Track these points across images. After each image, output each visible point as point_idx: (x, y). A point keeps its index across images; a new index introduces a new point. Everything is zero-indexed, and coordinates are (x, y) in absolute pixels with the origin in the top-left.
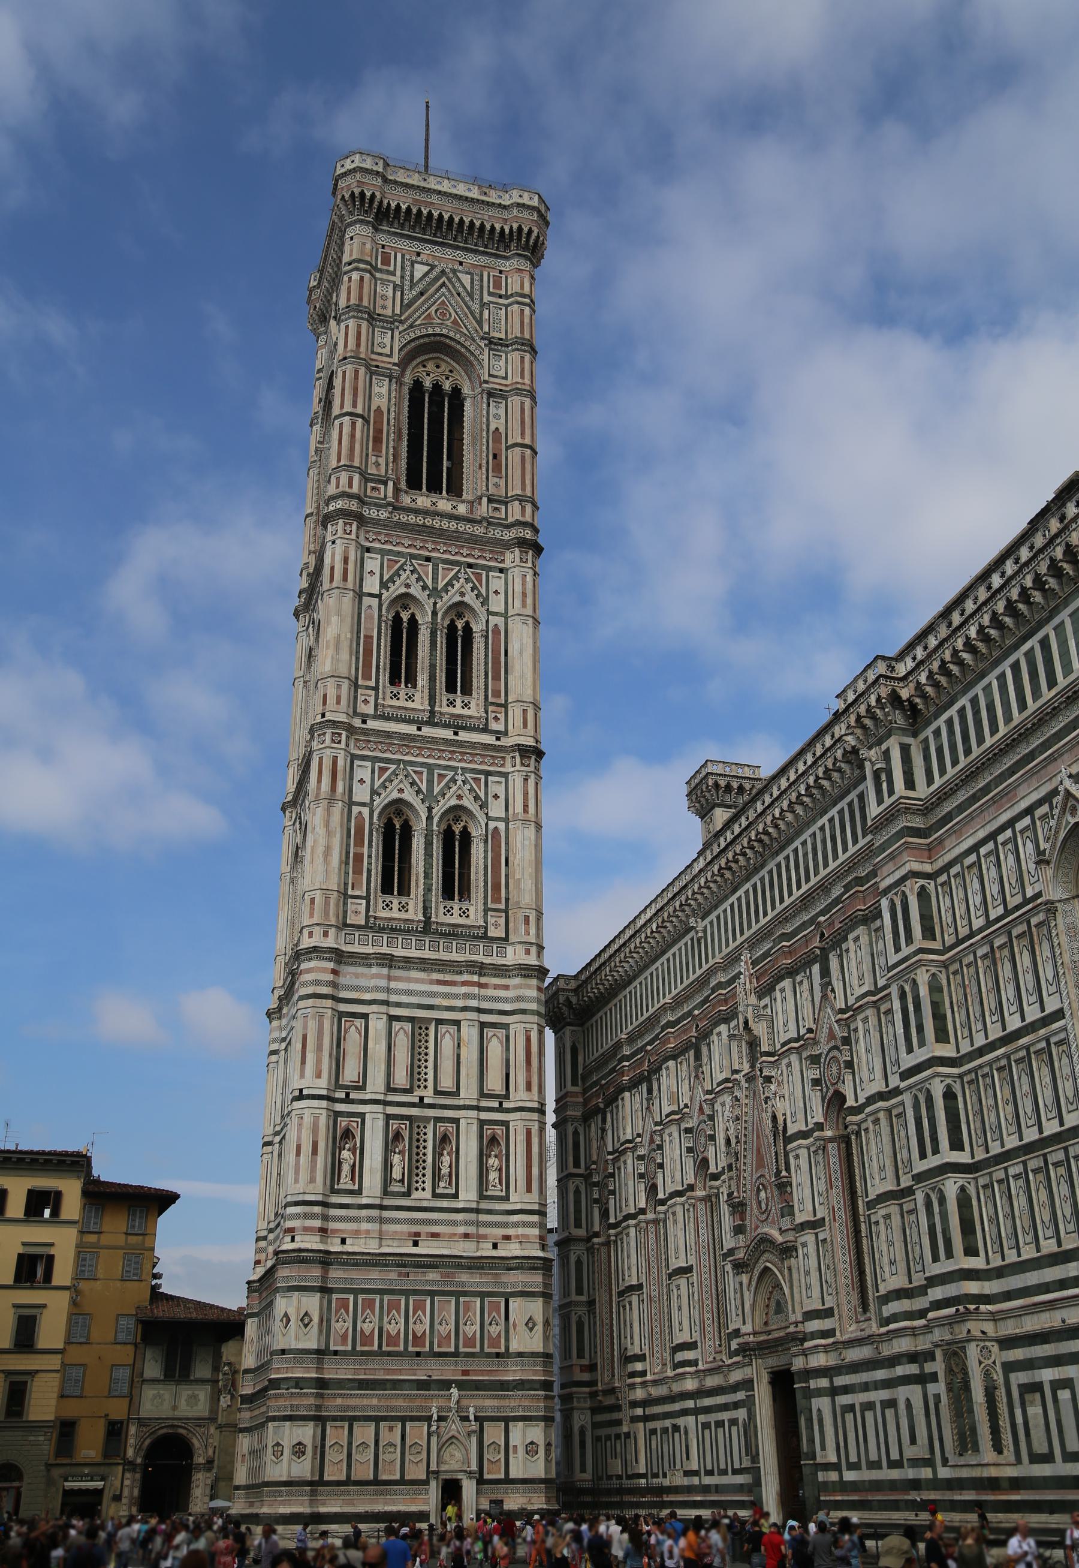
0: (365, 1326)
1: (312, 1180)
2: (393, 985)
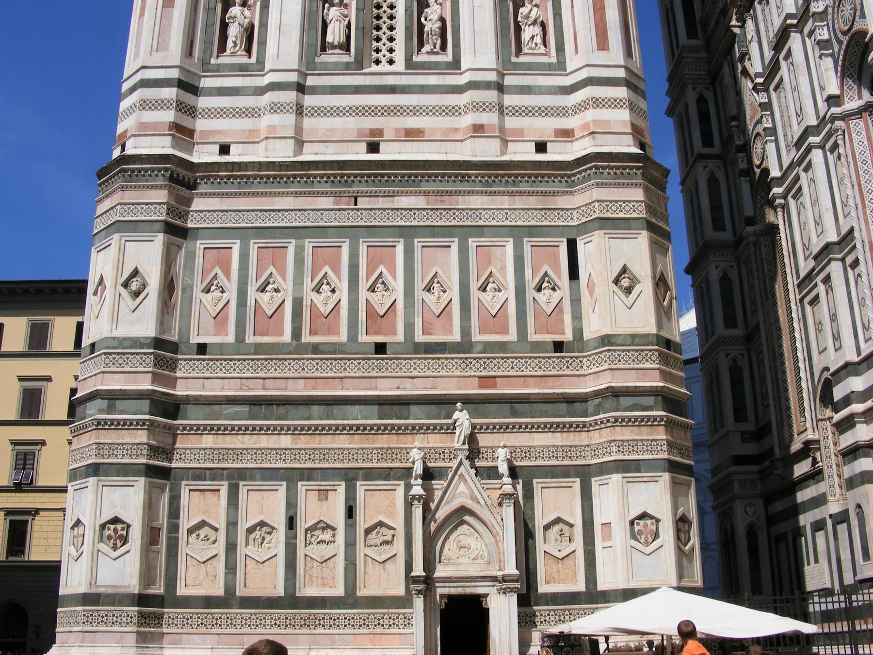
0: (265, 298)
1: (161, 46)
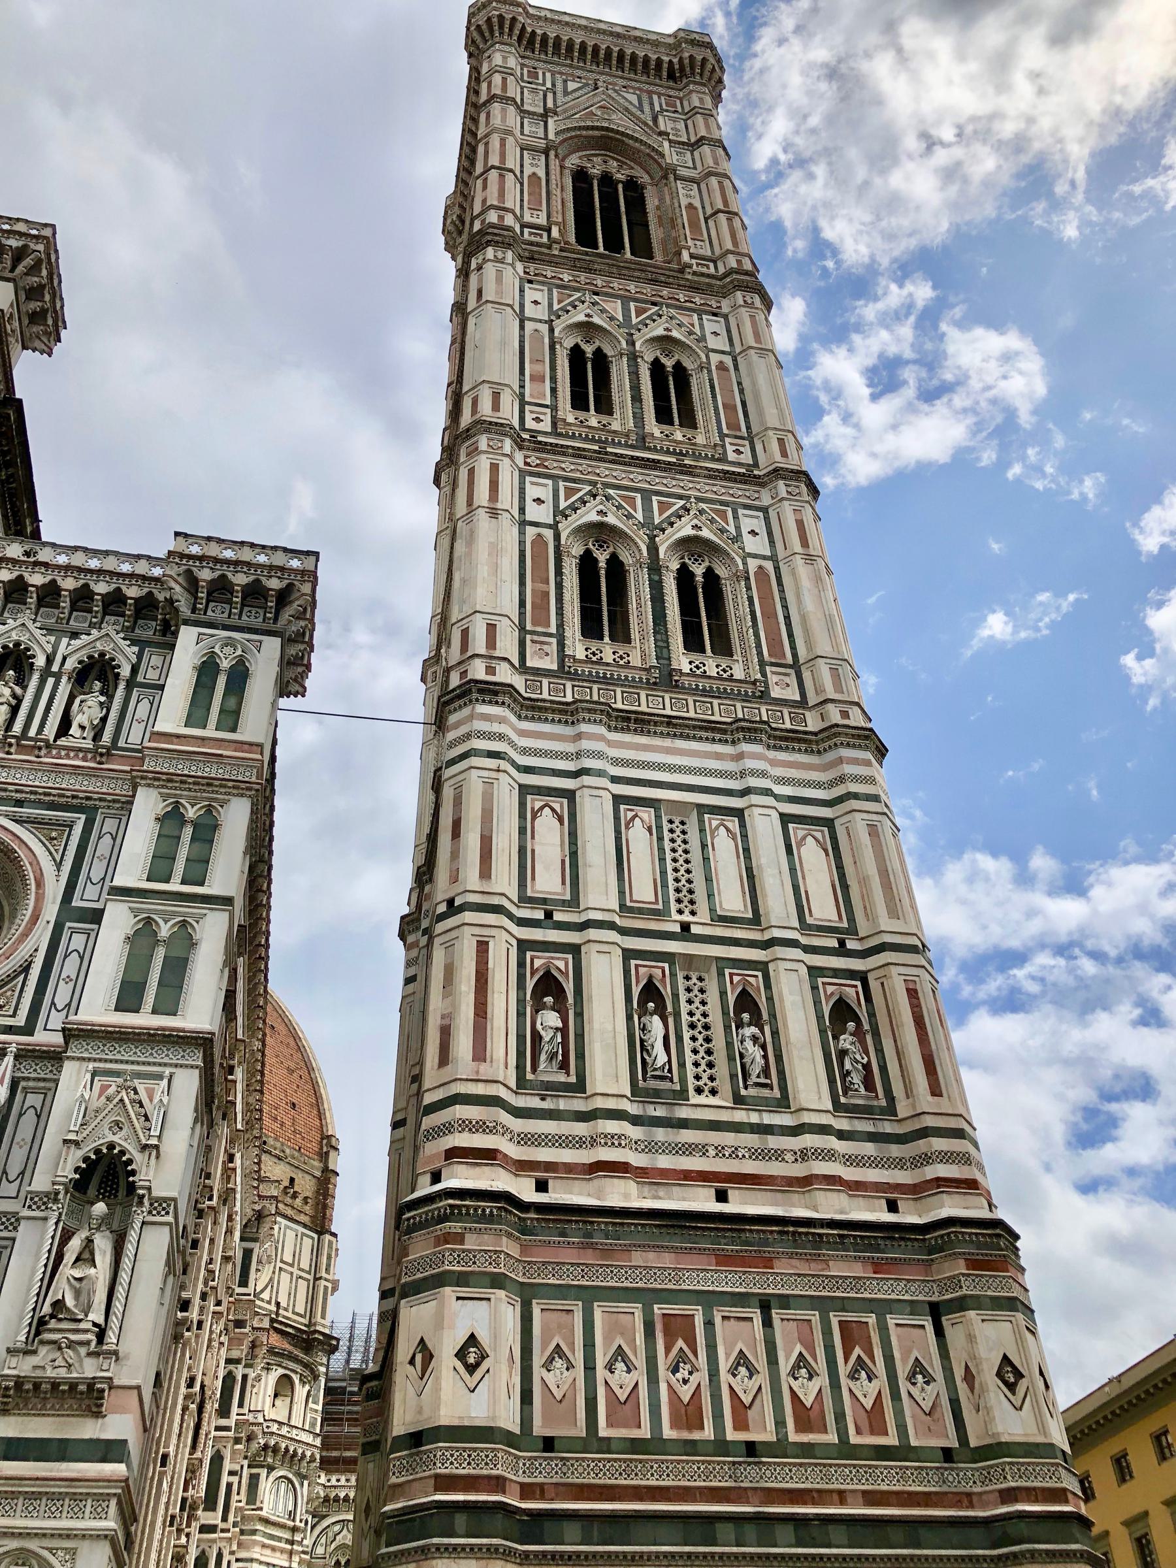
2: (613, 753)
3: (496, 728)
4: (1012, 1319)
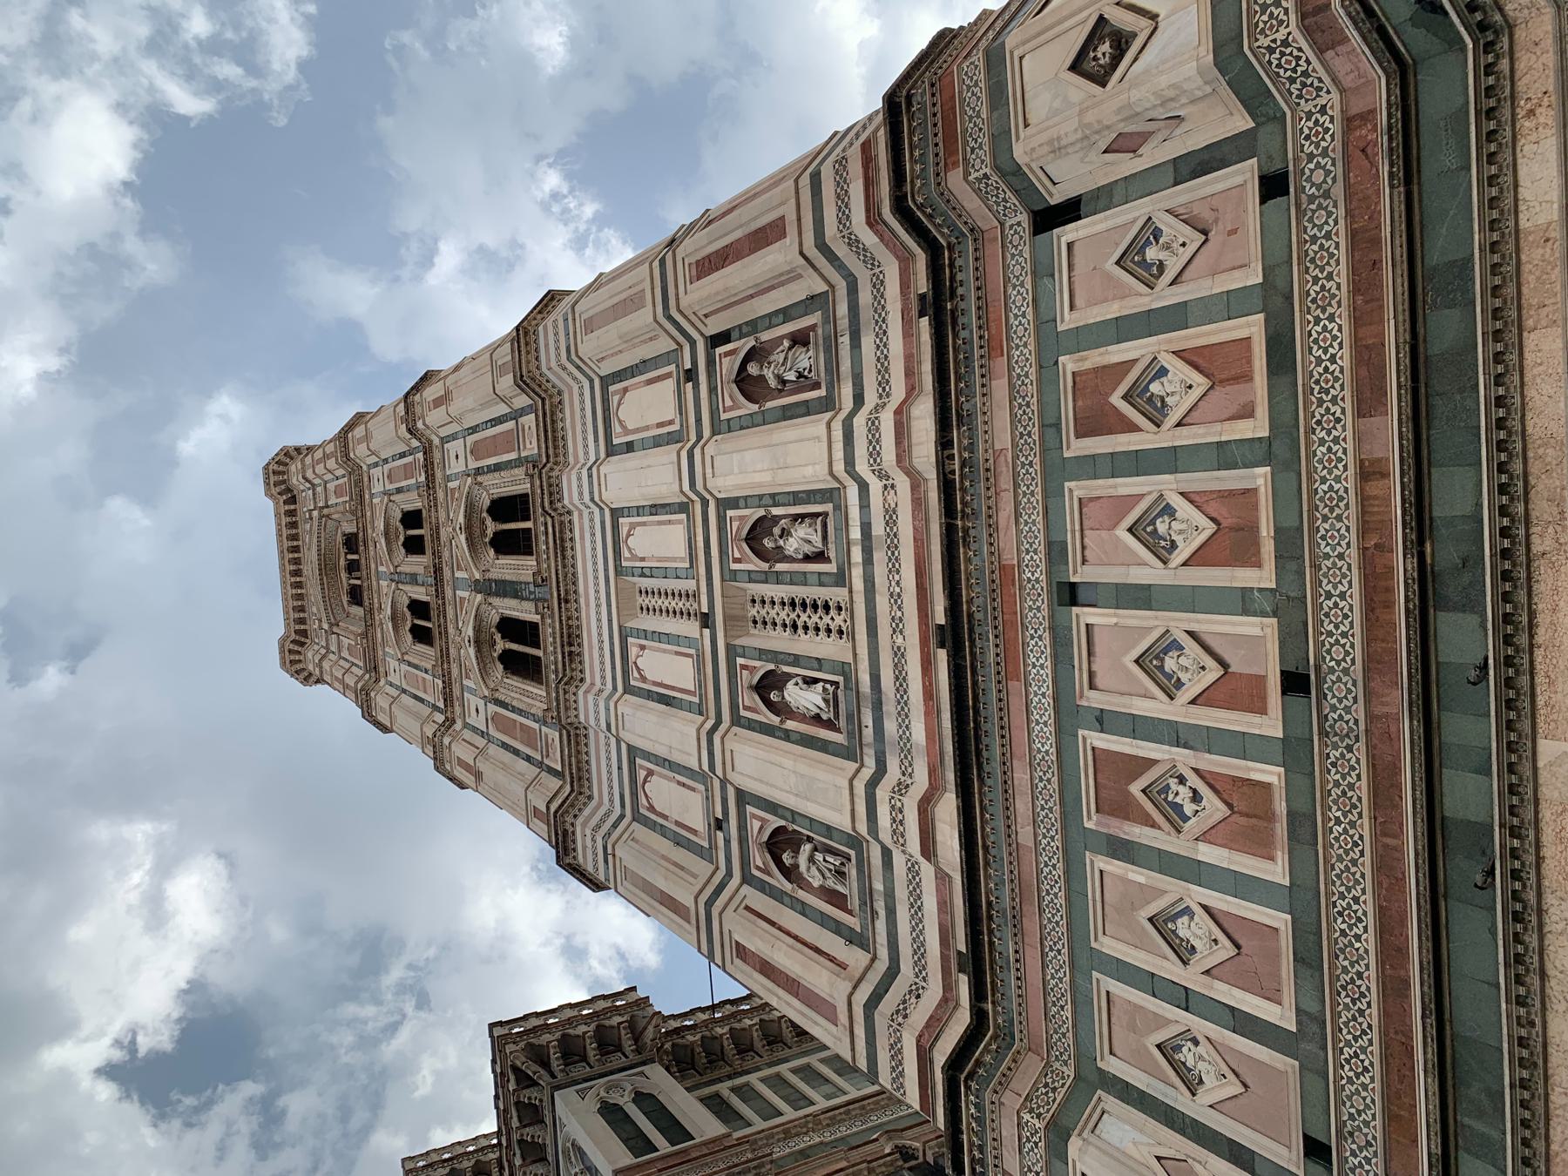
3: (589, 843)
4: (1017, 54)
